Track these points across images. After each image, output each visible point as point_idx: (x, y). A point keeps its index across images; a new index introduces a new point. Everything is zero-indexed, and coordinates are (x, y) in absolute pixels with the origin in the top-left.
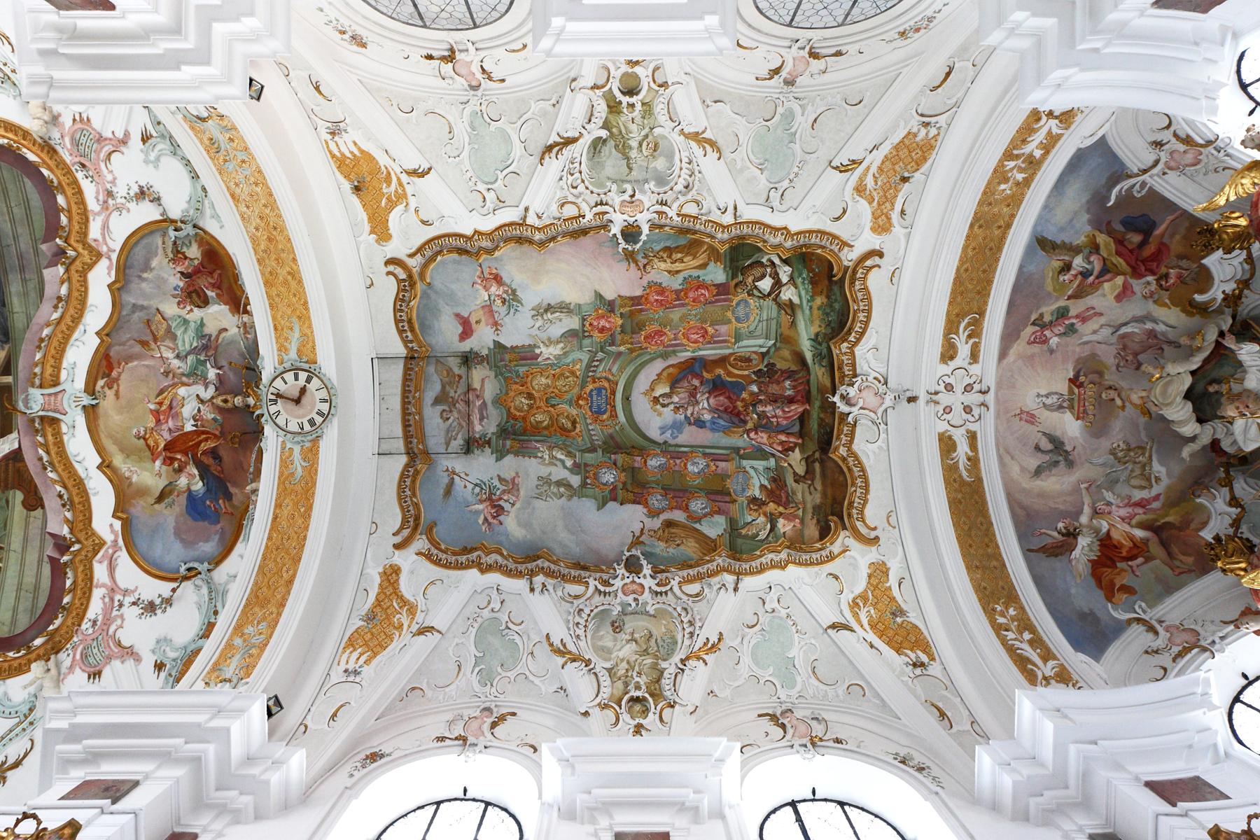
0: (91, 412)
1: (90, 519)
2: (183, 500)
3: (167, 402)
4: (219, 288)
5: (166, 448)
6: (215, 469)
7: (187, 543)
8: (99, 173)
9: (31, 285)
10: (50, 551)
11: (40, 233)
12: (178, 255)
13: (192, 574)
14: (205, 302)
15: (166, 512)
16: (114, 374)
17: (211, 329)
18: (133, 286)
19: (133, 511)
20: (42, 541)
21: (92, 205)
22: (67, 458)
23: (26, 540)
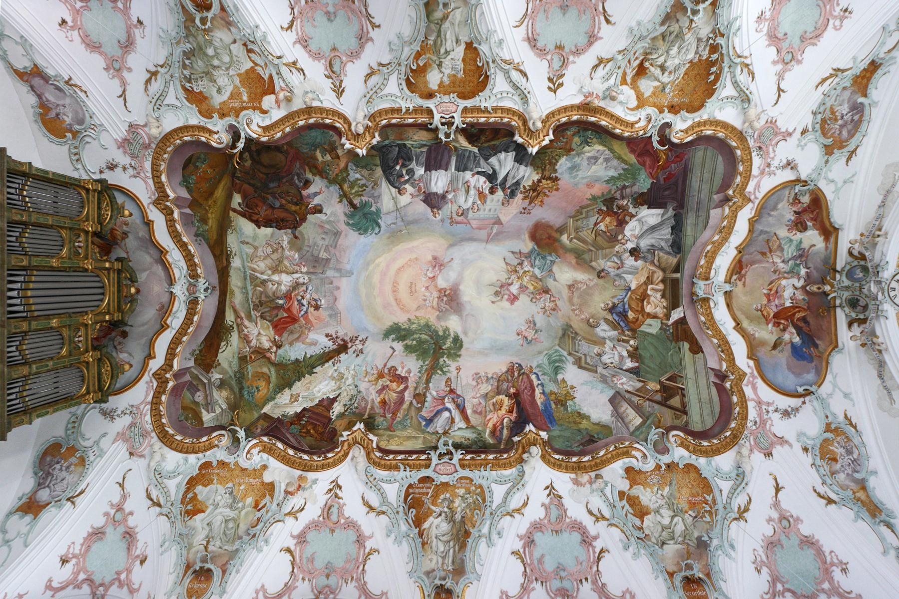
0: (727, 294)
1: (734, 359)
2: (789, 347)
3: (774, 289)
4: (815, 220)
5: (774, 317)
6: (806, 329)
7: (797, 375)
8: (768, 153)
9: (701, 219)
10: (713, 379)
11: (715, 189)
12: (796, 200)
13: (808, 393)
14: (805, 229)
15: (780, 355)
16: (743, 272)
17: (806, 245)
18: (763, 219)
19: (758, 354)
20: (707, 373)
21: (755, 171)
22: (715, 322)
23: (696, 372)
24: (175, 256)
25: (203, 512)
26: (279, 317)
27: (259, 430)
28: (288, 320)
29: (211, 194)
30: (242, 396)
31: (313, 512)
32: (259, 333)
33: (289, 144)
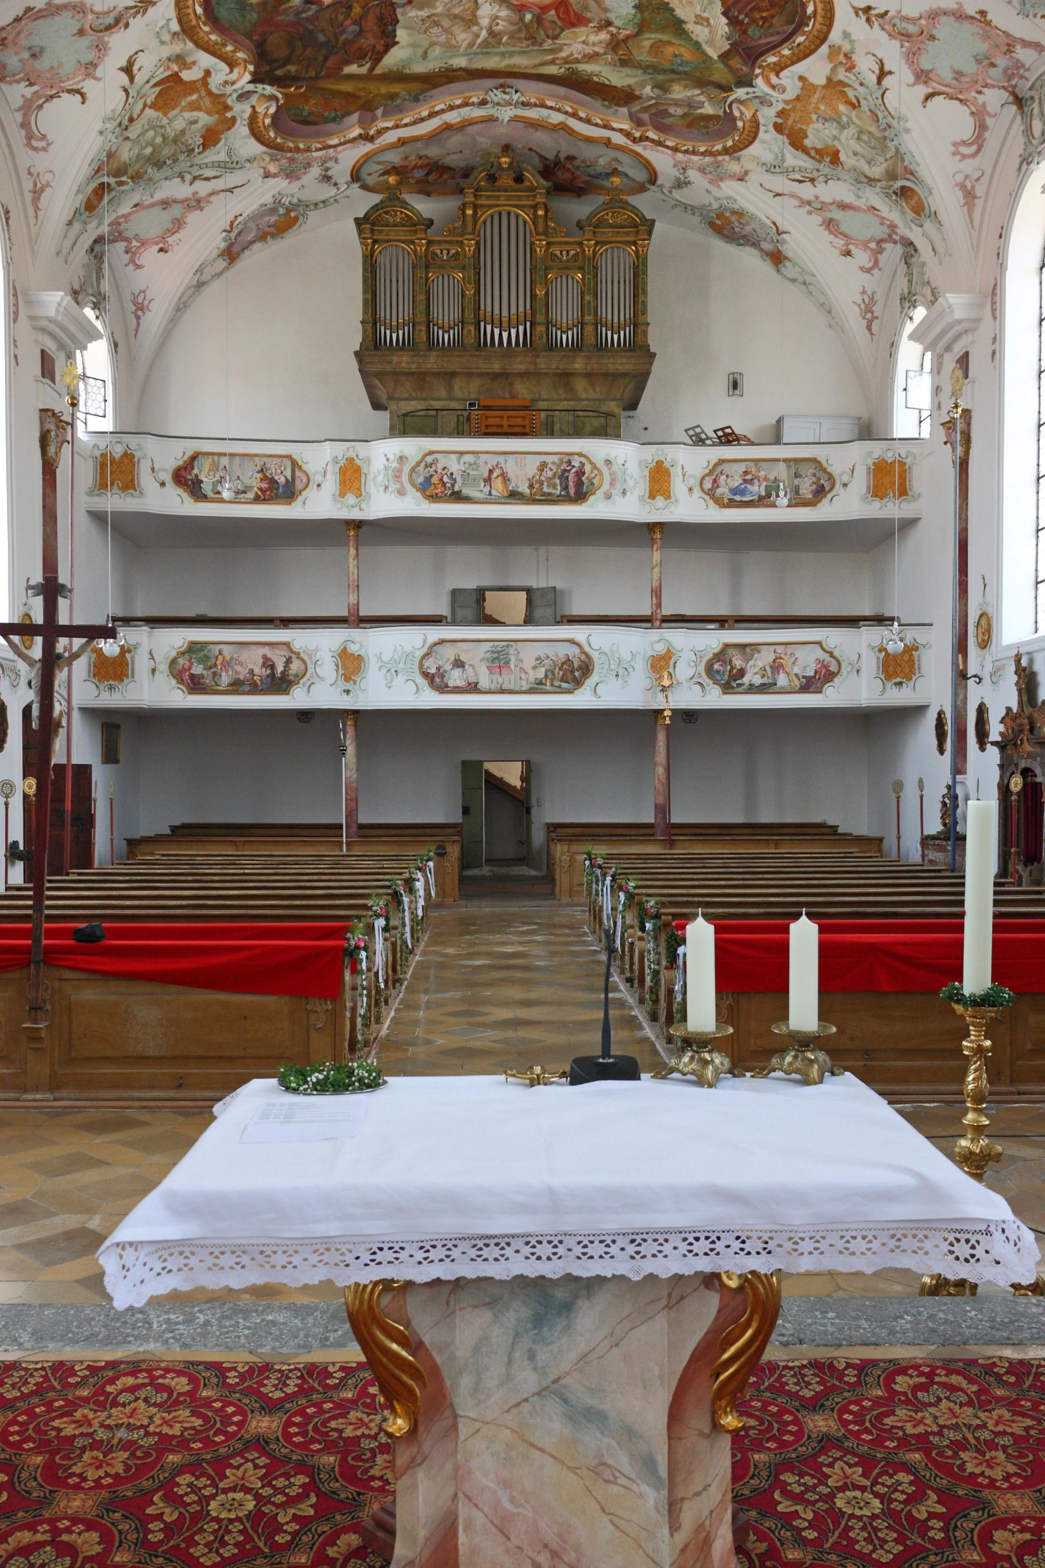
24: (452, 117)
25: (838, 152)
26: (556, 19)
27: (744, 68)
28: (562, 10)
29: (348, 94)
30: (685, 73)
31: (892, 52)
32: (583, 42)
33: (248, 35)
